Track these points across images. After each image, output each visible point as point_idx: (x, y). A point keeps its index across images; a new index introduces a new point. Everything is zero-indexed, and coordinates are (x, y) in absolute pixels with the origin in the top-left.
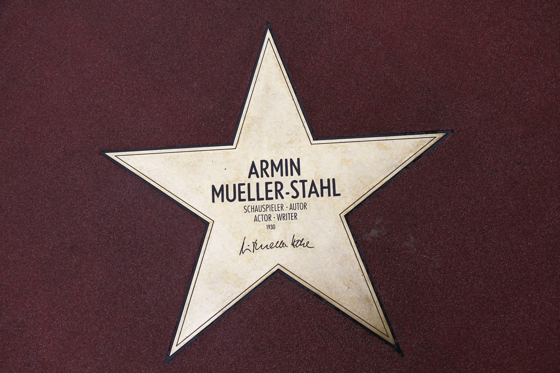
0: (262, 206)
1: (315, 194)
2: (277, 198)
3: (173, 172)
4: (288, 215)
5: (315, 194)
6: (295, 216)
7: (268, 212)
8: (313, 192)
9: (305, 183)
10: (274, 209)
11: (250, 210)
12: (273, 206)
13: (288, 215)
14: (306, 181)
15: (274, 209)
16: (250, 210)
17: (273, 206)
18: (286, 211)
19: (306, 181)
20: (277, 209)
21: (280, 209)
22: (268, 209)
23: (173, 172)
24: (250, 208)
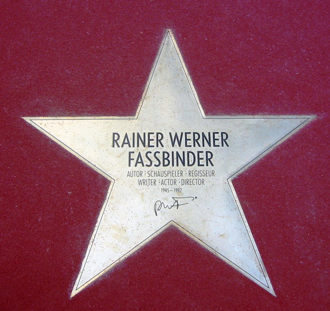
0: (164, 172)
1: (141, 164)
2: (207, 165)
3: (80, 136)
4: (148, 181)
5: (141, 164)
6: (154, 182)
8: (140, 163)
10: (174, 175)
11: (153, 174)
12: (174, 172)
13: (148, 181)
16: (153, 174)
18: (145, 177)
21: (180, 175)
22: (169, 175)
23: (80, 136)
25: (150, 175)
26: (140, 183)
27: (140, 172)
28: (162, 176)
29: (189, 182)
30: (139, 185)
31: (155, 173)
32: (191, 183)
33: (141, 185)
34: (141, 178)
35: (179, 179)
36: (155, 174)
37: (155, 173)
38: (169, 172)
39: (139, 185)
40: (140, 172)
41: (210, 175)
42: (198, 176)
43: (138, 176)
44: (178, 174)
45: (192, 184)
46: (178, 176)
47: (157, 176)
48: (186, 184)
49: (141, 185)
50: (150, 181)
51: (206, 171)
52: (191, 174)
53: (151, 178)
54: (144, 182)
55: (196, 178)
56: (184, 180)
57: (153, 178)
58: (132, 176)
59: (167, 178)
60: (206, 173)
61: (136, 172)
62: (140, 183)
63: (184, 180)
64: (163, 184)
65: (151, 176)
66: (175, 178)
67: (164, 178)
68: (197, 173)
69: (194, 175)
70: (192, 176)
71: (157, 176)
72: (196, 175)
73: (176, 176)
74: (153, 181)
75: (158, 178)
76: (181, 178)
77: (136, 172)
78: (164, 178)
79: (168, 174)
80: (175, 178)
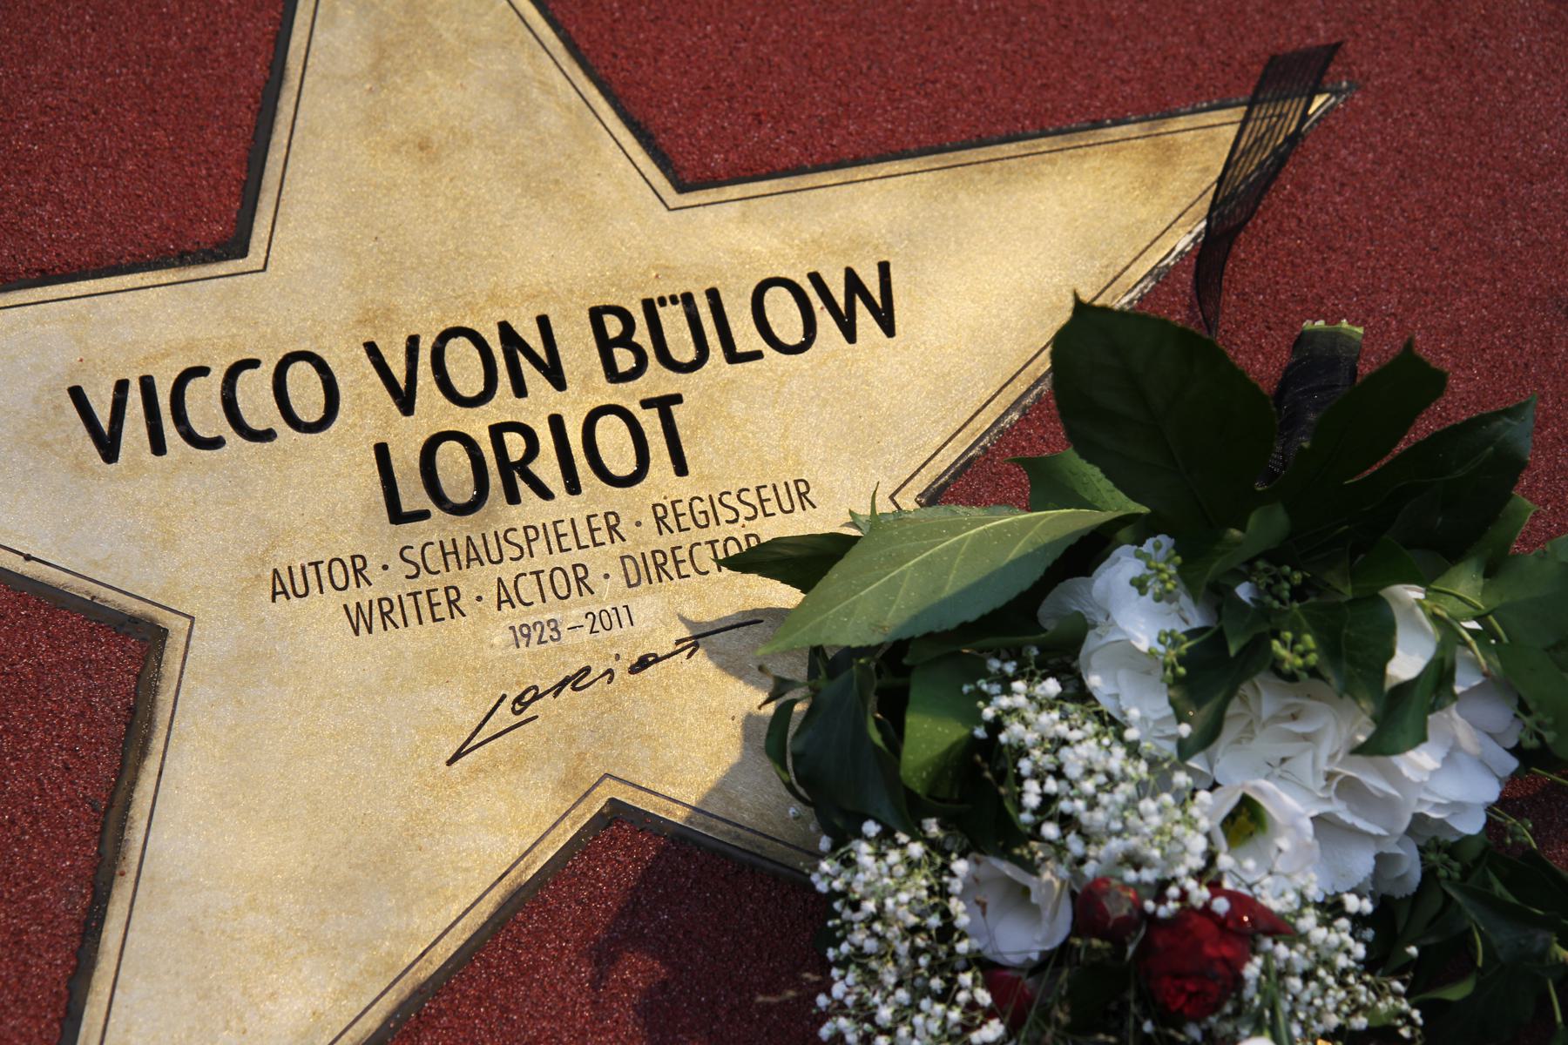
7: (541, 558)
9: (674, 408)
10: (568, 542)
12: (564, 528)
14: (677, 399)
15: (568, 542)
17: (564, 528)
19: (677, 399)
20: (585, 539)
21: (602, 536)
22: (539, 546)
24: (433, 554)
25: (420, 569)
26: (359, 620)
27: (349, 564)
28: (495, 557)
29: (670, 562)
30: (357, 632)
31: (449, 548)
32: (686, 568)
33: (370, 630)
34: (367, 594)
35: (603, 561)
36: (451, 559)
37: (449, 548)
38: (532, 533)
39: (357, 632)
40: (349, 564)
41: (787, 507)
42: (712, 521)
43: (341, 584)
44: (592, 531)
45: (692, 572)
46: (596, 545)
47: (464, 563)
48: (654, 576)
49: (370, 630)
50: (422, 598)
51: (758, 489)
52: (670, 520)
53: (424, 582)
54: (384, 615)
55: (713, 532)
56: (639, 560)
57: (438, 582)
58: (301, 590)
59: (526, 565)
60: (762, 501)
61: (323, 568)
62: (359, 620)
63: (639, 560)
64: (510, 600)
65: (422, 569)
66: (577, 556)
67: (508, 571)
68: (707, 506)
69: (686, 521)
70: (675, 529)
71: (464, 563)
72: (702, 520)
73: (580, 547)
74: (439, 597)
75: (478, 580)
76: (617, 549)
77: (323, 568)
78: (508, 571)
79: (529, 541)
80: (577, 556)
